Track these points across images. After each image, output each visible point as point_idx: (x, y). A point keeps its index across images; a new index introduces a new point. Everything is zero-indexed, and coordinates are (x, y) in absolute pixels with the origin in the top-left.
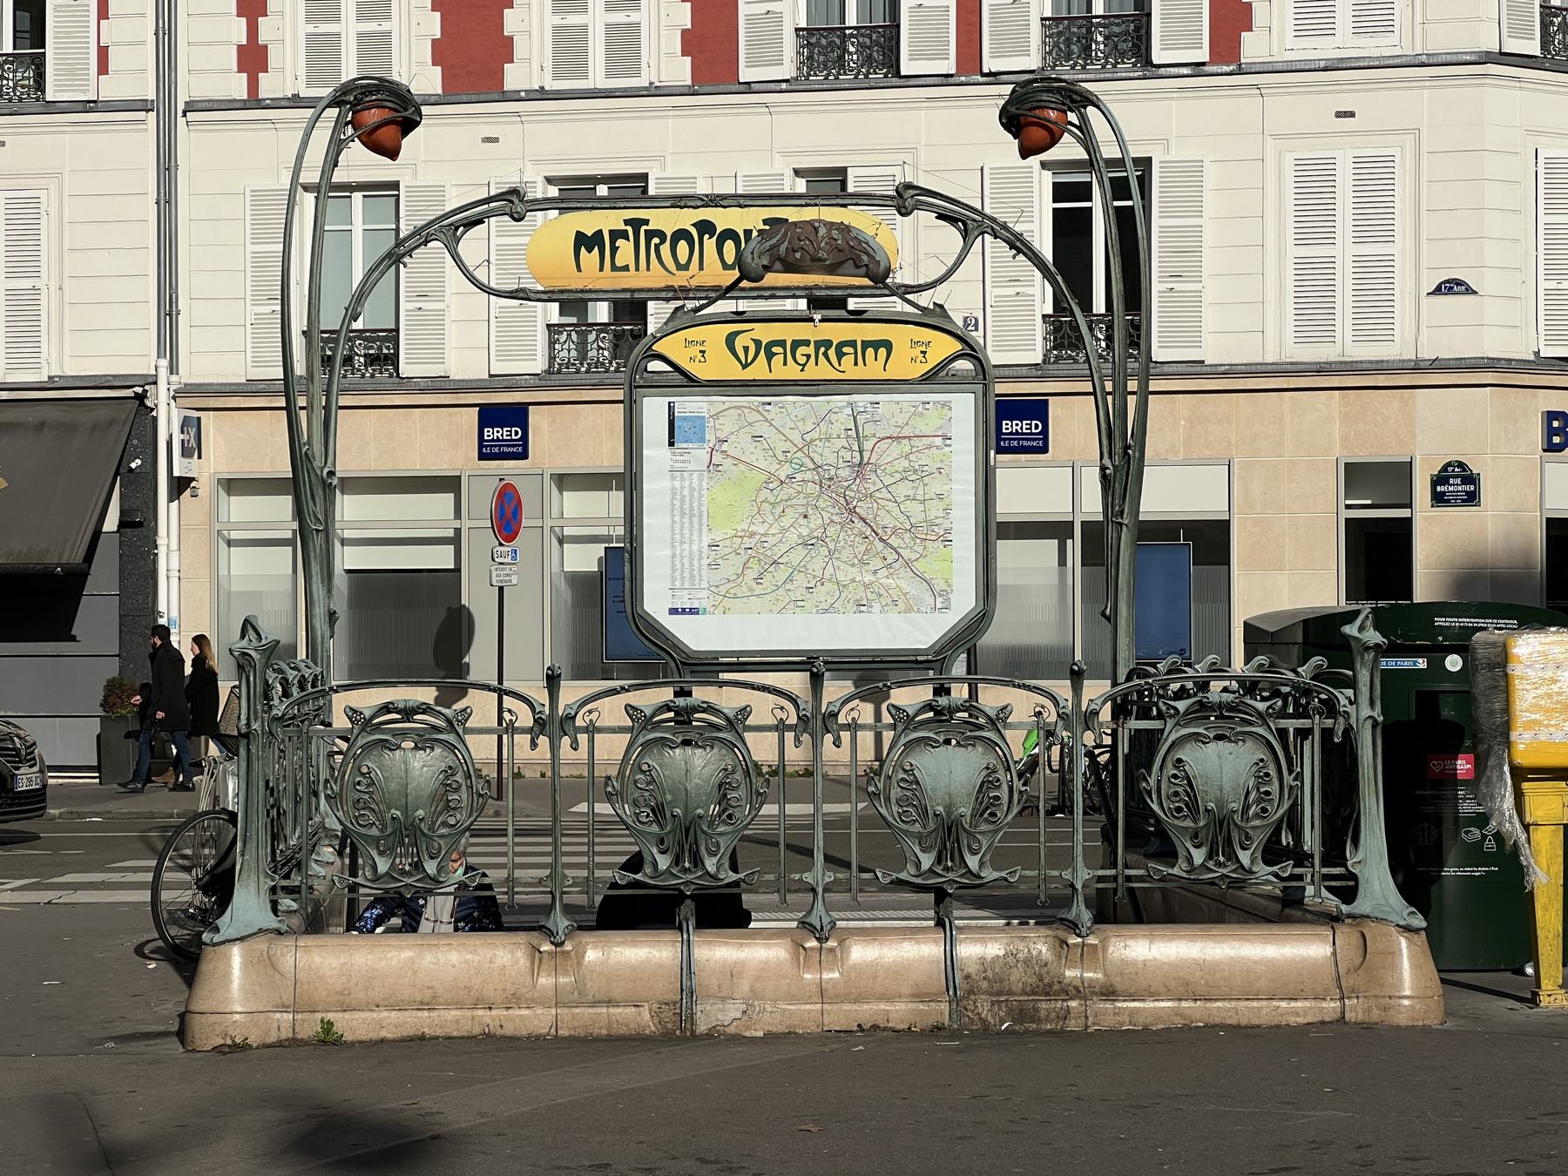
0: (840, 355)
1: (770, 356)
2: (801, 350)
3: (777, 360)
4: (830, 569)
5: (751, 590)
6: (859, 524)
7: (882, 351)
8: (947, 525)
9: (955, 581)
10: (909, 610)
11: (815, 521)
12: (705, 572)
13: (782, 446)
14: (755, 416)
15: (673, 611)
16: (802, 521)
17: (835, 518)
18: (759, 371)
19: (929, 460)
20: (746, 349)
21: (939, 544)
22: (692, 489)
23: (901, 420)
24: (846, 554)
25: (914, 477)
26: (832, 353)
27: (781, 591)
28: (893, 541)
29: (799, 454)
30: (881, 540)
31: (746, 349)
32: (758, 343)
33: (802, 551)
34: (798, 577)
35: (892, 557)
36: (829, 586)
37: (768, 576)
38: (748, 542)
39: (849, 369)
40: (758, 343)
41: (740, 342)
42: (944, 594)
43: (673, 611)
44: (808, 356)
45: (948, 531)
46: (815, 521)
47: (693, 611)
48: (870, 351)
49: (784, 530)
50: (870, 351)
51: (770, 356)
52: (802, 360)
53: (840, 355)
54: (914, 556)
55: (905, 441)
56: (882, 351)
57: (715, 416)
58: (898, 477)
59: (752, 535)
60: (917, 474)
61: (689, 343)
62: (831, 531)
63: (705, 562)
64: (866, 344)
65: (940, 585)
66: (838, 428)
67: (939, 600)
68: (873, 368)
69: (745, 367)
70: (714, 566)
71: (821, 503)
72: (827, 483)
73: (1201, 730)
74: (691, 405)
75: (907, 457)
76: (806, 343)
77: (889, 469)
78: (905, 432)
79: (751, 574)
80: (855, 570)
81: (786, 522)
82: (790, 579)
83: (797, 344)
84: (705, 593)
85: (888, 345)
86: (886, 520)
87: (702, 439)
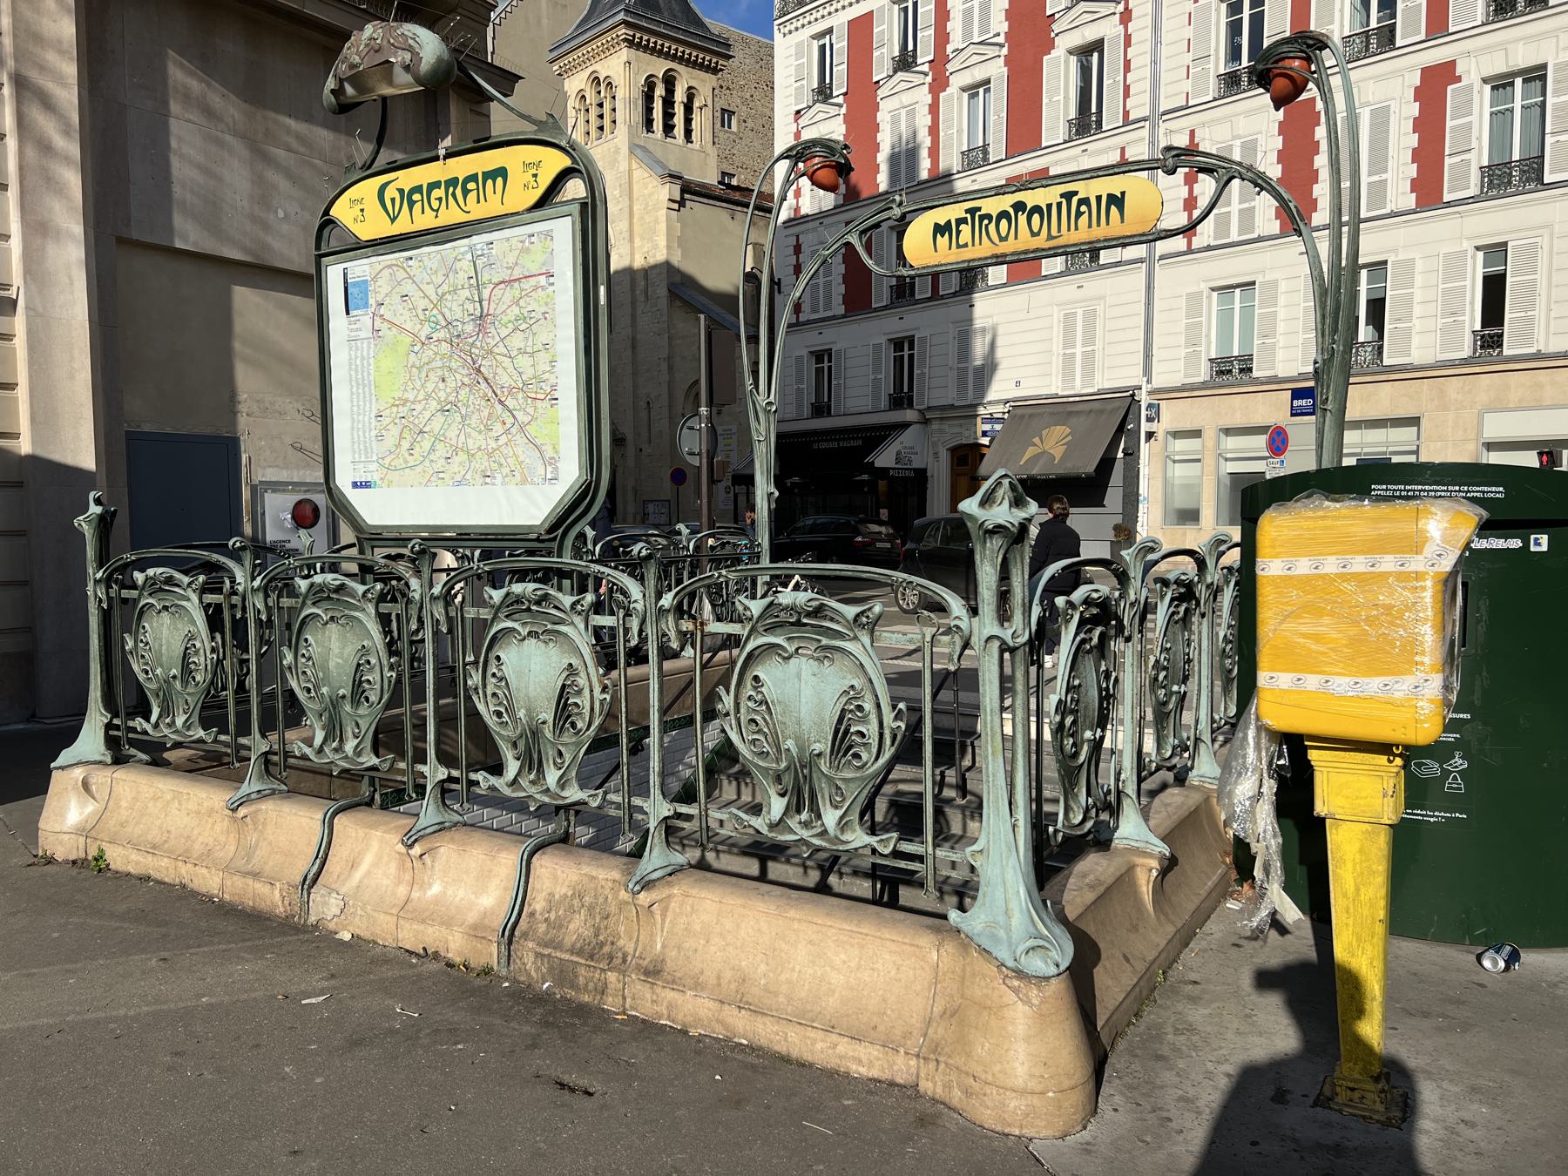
0: (466, 192)
1: (411, 204)
2: (436, 193)
3: (418, 206)
4: (462, 438)
5: (406, 461)
6: (484, 385)
7: (499, 180)
8: (553, 380)
9: (561, 448)
10: (524, 481)
11: (451, 383)
12: (374, 444)
13: (423, 303)
14: (401, 274)
15: (355, 485)
16: (441, 385)
17: (466, 380)
18: (403, 225)
19: (535, 305)
20: (393, 200)
21: (546, 404)
22: (363, 358)
23: (511, 259)
24: (474, 421)
25: (523, 326)
26: (459, 192)
27: (427, 463)
28: (510, 403)
29: (435, 312)
30: (501, 402)
31: (393, 200)
32: (401, 191)
33: (440, 418)
34: (439, 446)
35: (510, 420)
36: (462, 456)
37: (417, 448)
38: (403, 411)
39: (476, 210)
40: (401, 191)
41: (391, 192)
42: (551, 462)
43: (355, 485)
44: (440, 199)
45: (554, 388)
46: (451, 383)
47: (365, 485)
48: (490, 182)
49: (428, 397)
50: (490, 182)
51: (411, 204)
52: (435, 204)
53: (466, 192)
54: (526, 419)
55: (516, 285)
56: (499, 180)
57: (375, 279)
58: (511, 326)
59: (407, 401)
60: (526, 323)
61: (353, 202)
62: (464, 393)
63: (374, 433)
64: (486, 175)
65: (549, 453)
66: (462, 276)
67: (549, 469)
68: (492, 206)
69: (393, 220)
70: (380, 437)
71: (454, 365)
72: (456, 340)
73: (779, 640)
74: (361, 268)
75: (517, 303)
76: (437, 185)
77: (505, 319)
78: (516, 275)
79: (406, 445)
80: (482, 437)
81: (430, 386)
82: (432, 449)
83: (434, 185)
84: (373, 467)
85: (502, 172)
86: (504, 379)
87: (366, 305)
